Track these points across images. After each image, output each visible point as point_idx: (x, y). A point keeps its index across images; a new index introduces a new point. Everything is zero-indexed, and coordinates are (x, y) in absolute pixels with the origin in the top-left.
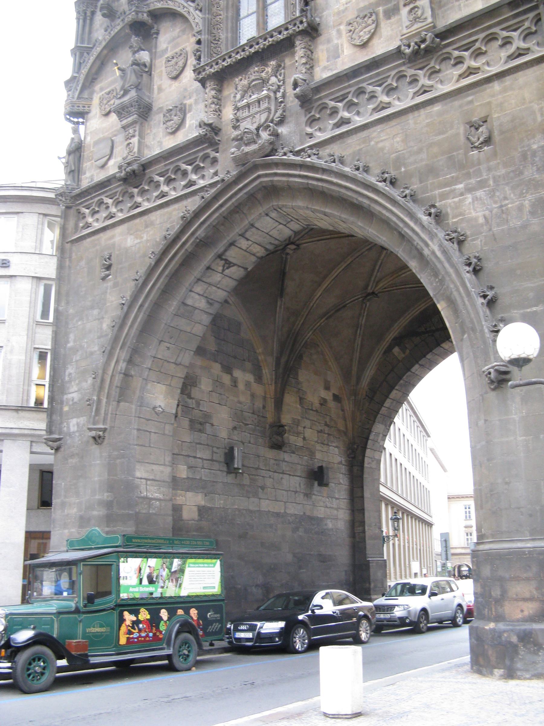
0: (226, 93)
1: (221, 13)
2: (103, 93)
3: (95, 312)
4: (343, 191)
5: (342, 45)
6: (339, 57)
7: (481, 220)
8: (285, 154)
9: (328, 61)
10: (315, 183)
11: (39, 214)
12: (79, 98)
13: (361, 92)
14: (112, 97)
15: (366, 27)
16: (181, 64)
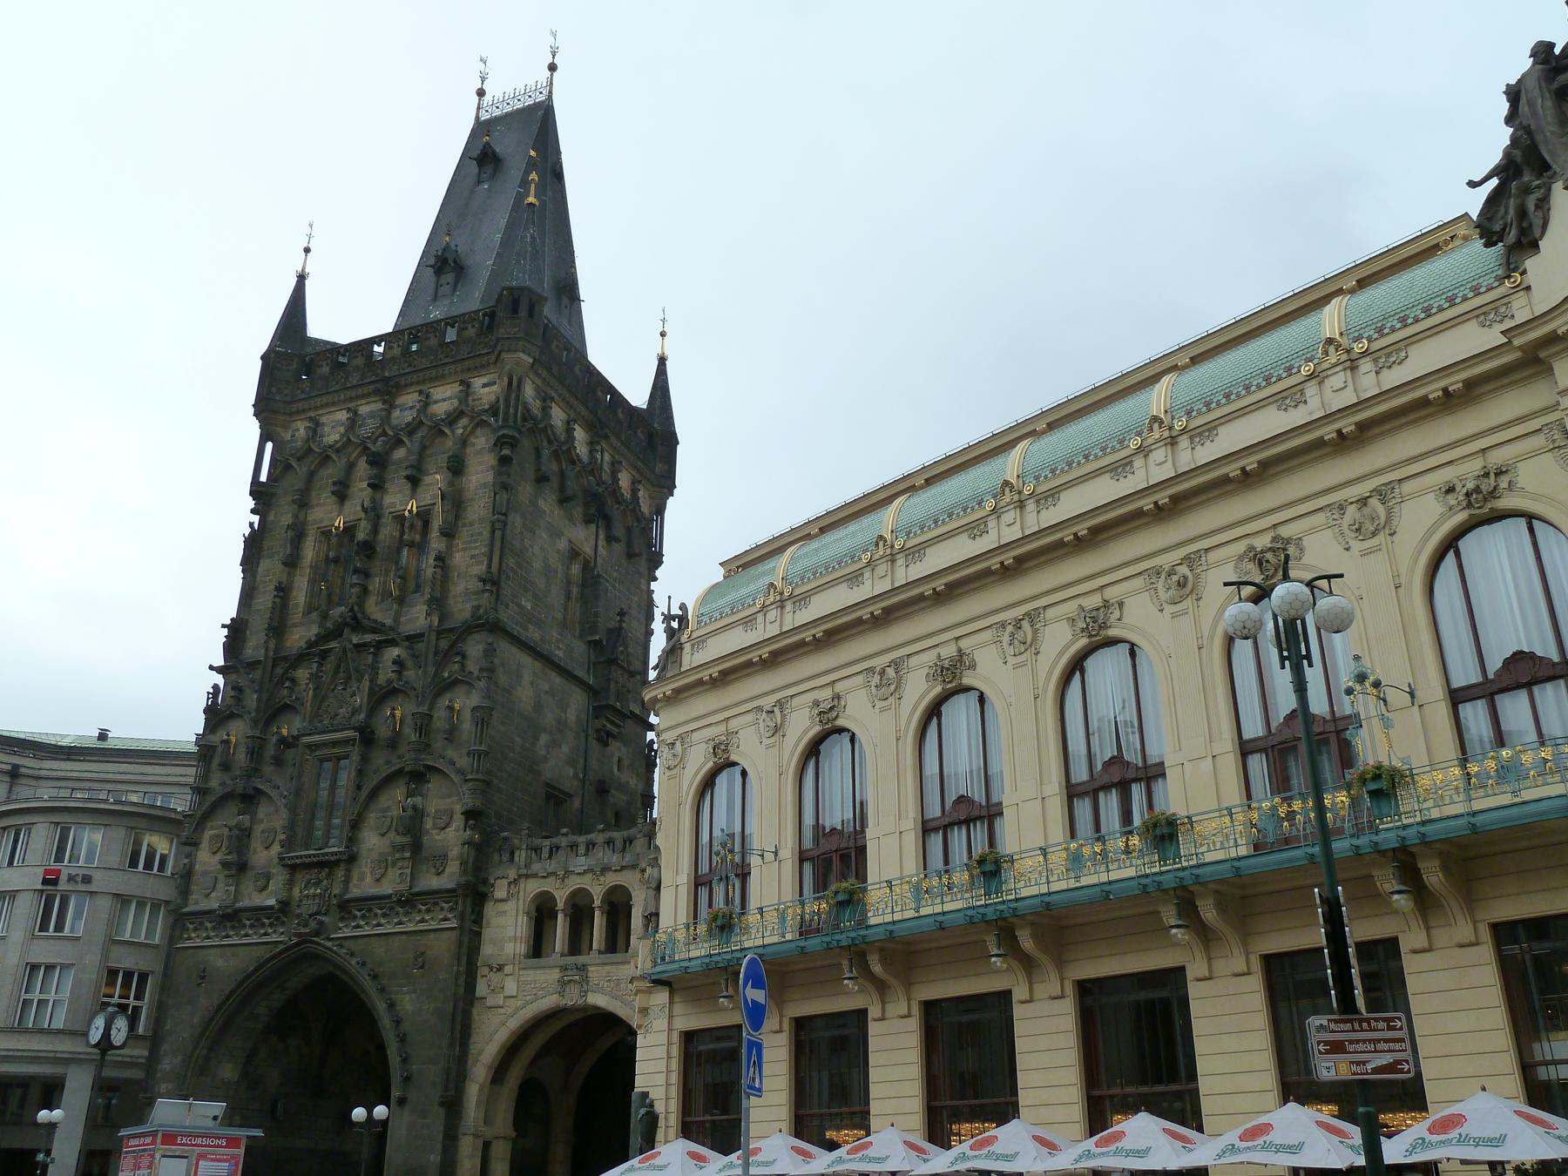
2: (212, 832)
11: (128, 827)
12: (193, 832)
13: (370, 910)
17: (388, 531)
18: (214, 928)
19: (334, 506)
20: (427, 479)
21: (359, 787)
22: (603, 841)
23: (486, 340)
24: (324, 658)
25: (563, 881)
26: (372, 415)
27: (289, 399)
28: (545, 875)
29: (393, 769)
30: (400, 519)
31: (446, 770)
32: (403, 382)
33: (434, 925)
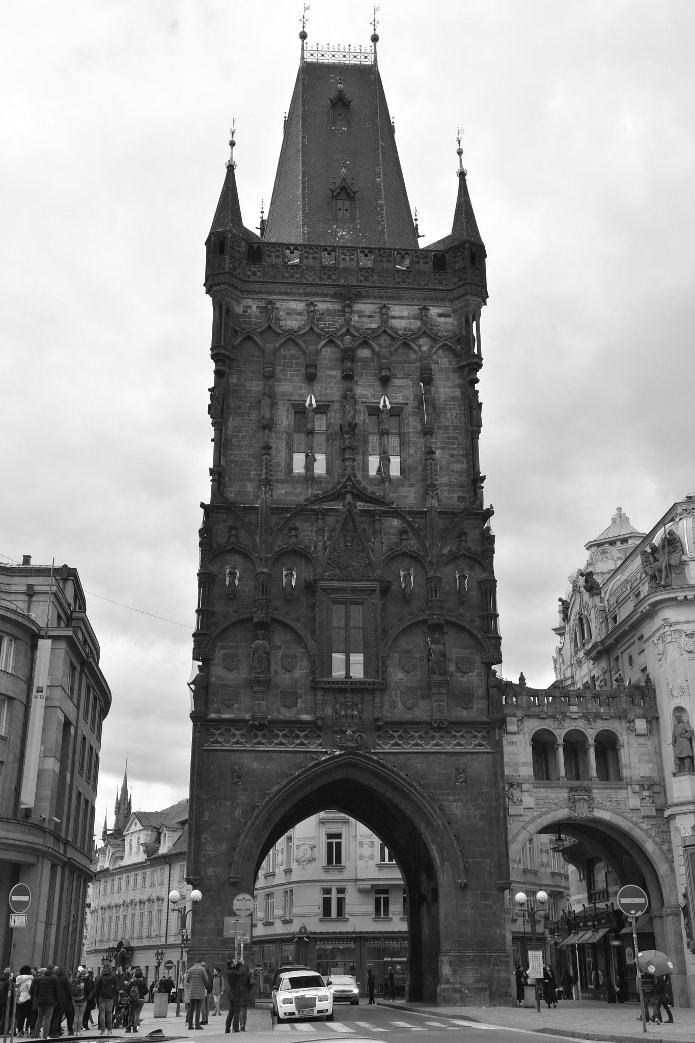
0: (326, 697)
3: (228, 803)
4: (395, 781)
5: (398, 702)
7: (459, 816)
8: (368, 753)
10: (380, 772)
12: (209, 649)
13: (406, 732)
14: (236, 660)
17: (362, 418)
18: (242, 735)
19: (303, 385)
20: (397, 382)
21: (384, 631)
22: (590, 695)
23: (439, 278)
25: (560, 723)
26: (328, 312)
27: (241, 276)
28: (545, 716)
29: (417, 620)
30: (375, 411)
31: (468, 627)
32: (363, 291)
33: (470, 749)
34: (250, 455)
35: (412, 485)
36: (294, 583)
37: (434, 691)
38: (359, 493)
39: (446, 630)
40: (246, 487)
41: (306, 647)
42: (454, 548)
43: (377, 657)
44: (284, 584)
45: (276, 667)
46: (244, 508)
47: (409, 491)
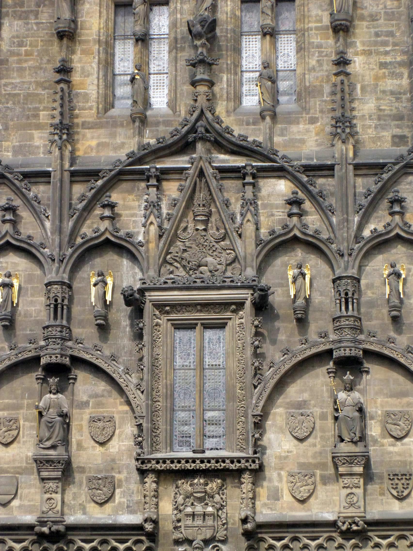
1: (161, 399)
5: (282, 490)
6: (278, 500)
9: (268, 500)
14: (14, 427)
15: (306, 485)
16: (109, 431)
21: (257, 371)
24: (159, 180)
29: (314, 350)
31: (402, 360)
34: (38, 84)
35: (313, 121)
36: (109, 298)
37: (342, 470)
38: (219, 139)
39: (366, 365)
40: (31, 138)
41: (129, 403)
42: (380, 228)
43: (246, 417)
44: (93, 300)
45: (80, 438)
46: (26, 176)
47: (308, 131)
